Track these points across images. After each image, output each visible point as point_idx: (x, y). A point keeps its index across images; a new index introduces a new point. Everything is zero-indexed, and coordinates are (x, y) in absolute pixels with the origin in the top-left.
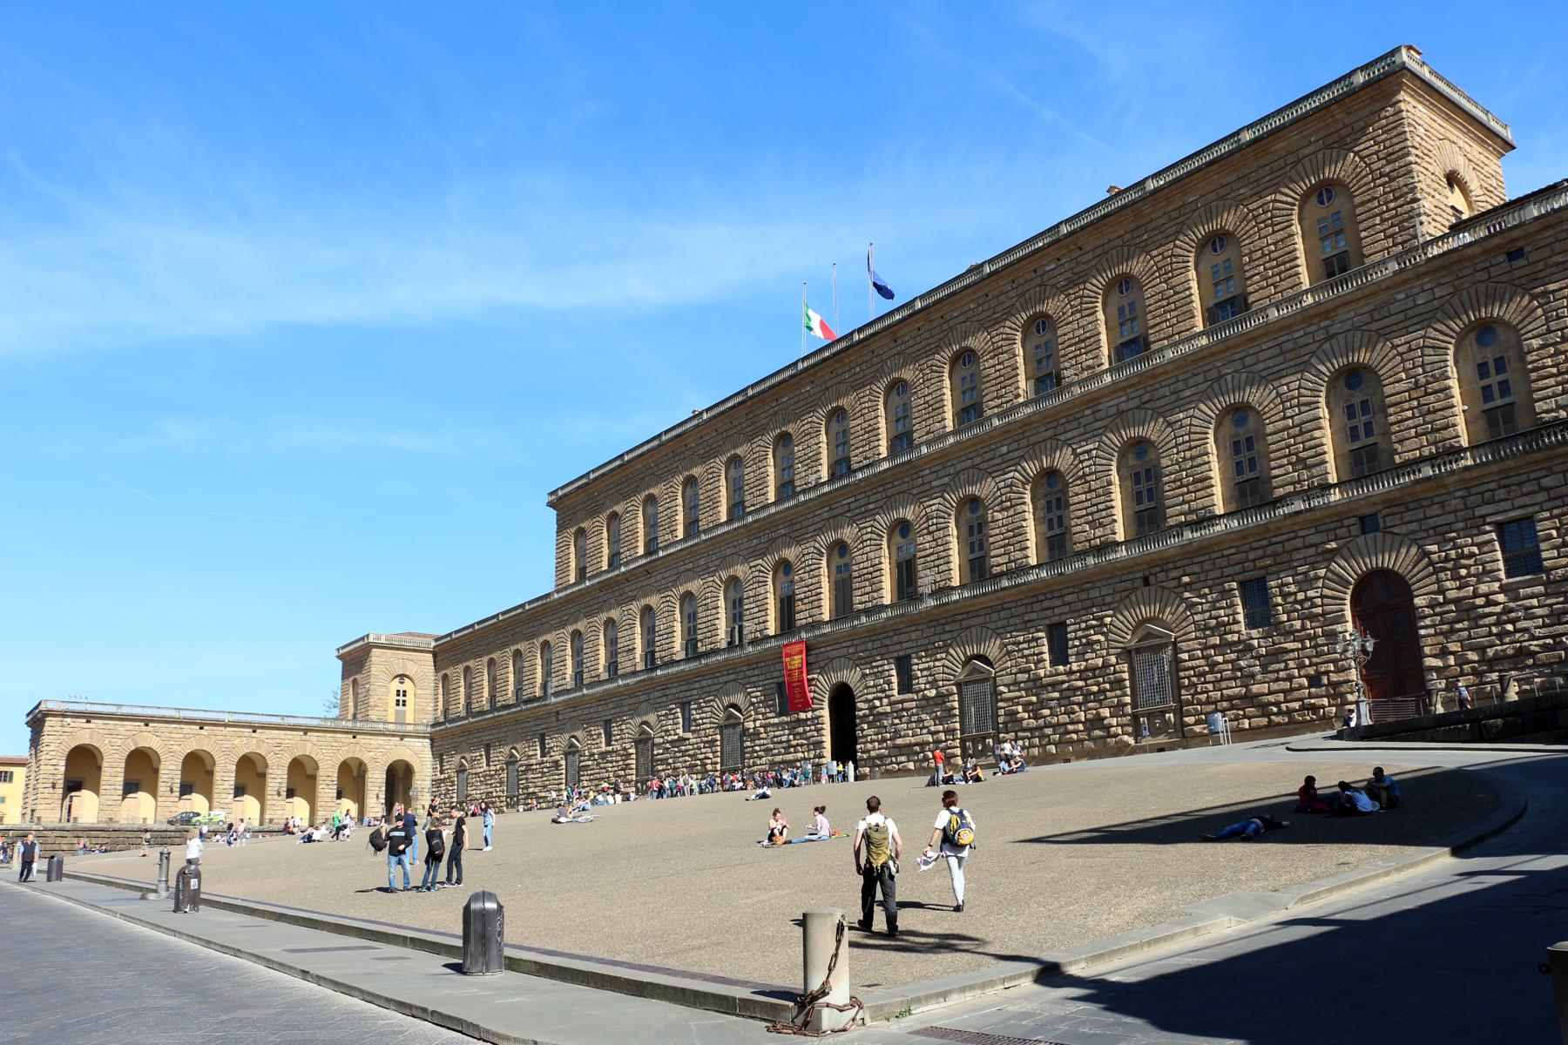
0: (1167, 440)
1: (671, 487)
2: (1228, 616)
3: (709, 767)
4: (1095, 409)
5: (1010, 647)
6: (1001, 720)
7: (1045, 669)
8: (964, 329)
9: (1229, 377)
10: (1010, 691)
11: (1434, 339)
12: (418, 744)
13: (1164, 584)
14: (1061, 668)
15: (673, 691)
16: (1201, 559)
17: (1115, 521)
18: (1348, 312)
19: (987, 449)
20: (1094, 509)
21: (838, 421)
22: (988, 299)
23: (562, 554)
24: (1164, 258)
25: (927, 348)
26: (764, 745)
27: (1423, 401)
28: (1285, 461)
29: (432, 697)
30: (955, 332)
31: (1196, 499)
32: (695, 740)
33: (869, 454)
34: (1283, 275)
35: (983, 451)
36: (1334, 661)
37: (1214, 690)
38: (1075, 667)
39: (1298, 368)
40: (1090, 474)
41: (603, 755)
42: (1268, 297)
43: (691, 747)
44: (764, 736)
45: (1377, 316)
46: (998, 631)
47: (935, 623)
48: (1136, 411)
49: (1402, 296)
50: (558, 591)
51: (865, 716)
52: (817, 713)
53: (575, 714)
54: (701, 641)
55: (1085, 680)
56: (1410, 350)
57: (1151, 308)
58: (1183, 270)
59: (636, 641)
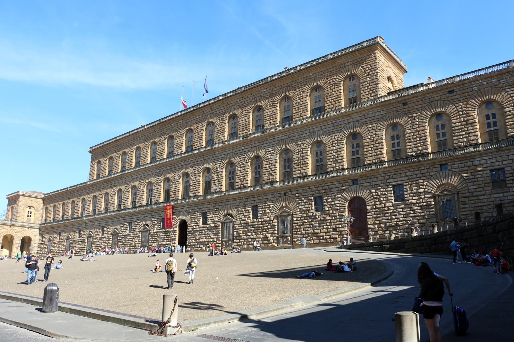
0: (296, 150)
1: (132, 150)
2: (310, 207)
3: (137, 245)
4: (274, 138)
5: (239, 212)
6: (235, 235)
7: (250, 220)
8: (234, 107)
9: (317, 132)
10: (238, 226)
11: (380, 127)
12: (34, 231)
13: (290, 196)
14: (255, 220)
15: (127, 218)
16: (303, 189)
17: (277, 174)
18: (355, 115)
19: (238, 147)
20: (270, 170)
22: (243, 99)
23: (92, 169)
24: (300, 92)
25: (222, 112)
26: (156, 238)
27: (375, 145)
28: (331, 160)
29: (41, 215)
30: (231, 108)
31: (303, 170)
32: (132, 235)
33: (199, 145)
34: (336, 102)
35: (236, 148)
36: (341, 224)
37: (303, 231)
38: (260, 220)
39: (338, 131)
40: (270, 158)
41: (101, 238)
42: (331, 108)
43: (131, 238)
44: (156, 235)
45: (363, 118)
46: (236, 207)
47: (215, 202)
48: (287, 140)
49: (371, 112)
50: (89, 182)
51: (190, 231)
52: (174, 229)
53: (92, 224)
54: (137, 202)
55: (263, 224)
56: (372, 129)
57: (295, 107)
58: (306, 97)
59: (115, 200)
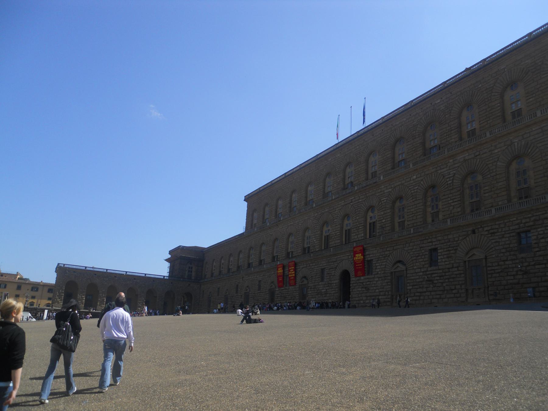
9: (516, 144)
21: (349, 168)
25: (385, 138)
46: (409, 251)
